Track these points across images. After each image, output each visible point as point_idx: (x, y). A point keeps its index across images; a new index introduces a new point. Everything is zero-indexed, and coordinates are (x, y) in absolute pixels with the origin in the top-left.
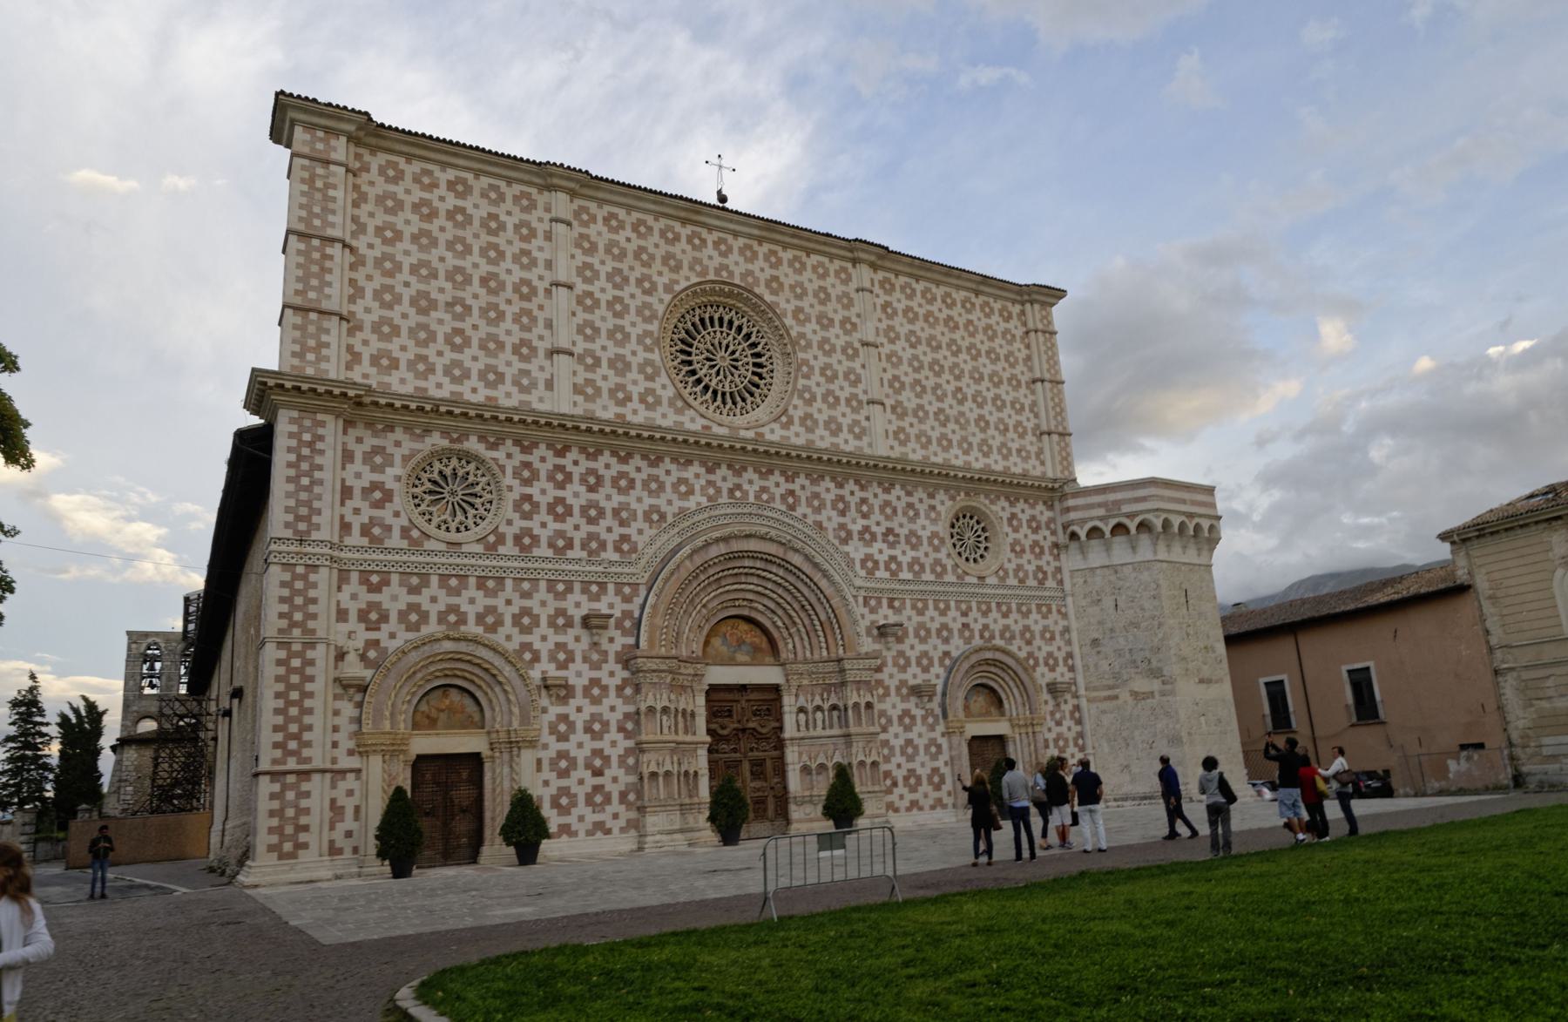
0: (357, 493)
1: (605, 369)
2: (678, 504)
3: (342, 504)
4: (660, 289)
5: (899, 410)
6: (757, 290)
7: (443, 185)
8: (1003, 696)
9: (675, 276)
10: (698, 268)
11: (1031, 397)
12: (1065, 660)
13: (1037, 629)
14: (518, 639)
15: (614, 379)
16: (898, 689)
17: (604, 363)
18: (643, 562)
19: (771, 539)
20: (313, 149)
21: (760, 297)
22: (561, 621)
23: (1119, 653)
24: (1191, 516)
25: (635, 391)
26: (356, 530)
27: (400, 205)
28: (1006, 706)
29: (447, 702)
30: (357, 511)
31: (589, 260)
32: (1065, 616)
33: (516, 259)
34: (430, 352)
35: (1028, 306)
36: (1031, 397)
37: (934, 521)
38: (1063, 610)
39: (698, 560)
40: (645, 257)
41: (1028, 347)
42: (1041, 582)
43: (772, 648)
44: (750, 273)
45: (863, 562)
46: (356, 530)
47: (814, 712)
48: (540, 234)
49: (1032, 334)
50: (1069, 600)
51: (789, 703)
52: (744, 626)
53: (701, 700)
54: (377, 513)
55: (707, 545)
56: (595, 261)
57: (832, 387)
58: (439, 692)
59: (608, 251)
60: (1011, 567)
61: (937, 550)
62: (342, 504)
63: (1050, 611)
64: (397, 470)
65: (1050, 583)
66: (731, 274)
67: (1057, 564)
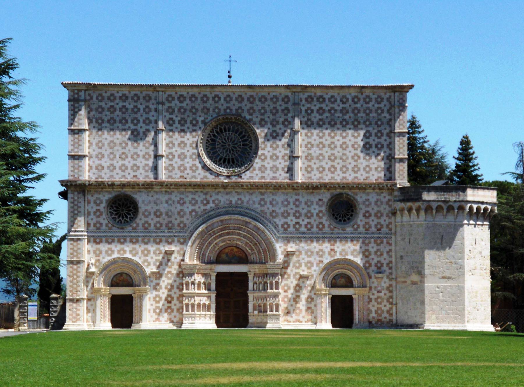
0: (92, 214)
1: (176, 159)
2: (203, 208)
3: (88, 217)
4: (200, 123)
5: (309, 158)
6: (243, 115)
7: (118, 98)
8: (353, 279)
9: (206, 116)
10: (217, 110)
11: (388, 140)
12: (388, 264)
13: (373, 250)
14: (143, 258)
15: (180, 163)
16: (294, 276)
17: (176, 157)
18: (189, 231)
19: (240, 220)
20: (74, 98)
21: (245, 117)
22: (158, 252)
23: (409, 262)
24: (445, 202)
25: (188, 166)
26: (92, 225)
27: (103, 109)
28: (354, 283)
29: (122, 278)
30: (92, 219)
31: (171, 116)
32: (390, 245)
33: (144, 122)
34: (115, 162)
35: (393, 94)
36: (388, 140)
37: (320, 206)
38: (390, 242)
39: (210, 229)
40: (194, 111)
41: (390, 114)
42: (379, 230)
43: (244, 260)
44: (240, 108)
45: (282, 226)
46: (92, 225)
47: (259, 284)
48: (153, 110)
49: (393, 108)
50: (393, 237)
51: (251, 278)
52: (235, 250)
53: (214, 278)
54: (98, 219)
55: (212, 224)
56: (173, 117)
57: (275, 152)
58: (119, 275)
59: (179, 110)
60: (361, 224)
61: (321, 218)
62: (88, 217)
63: (382, 242)
64: (104, 205)
65: (384, 229)
66: (231, 110)
67: (390, 220)
